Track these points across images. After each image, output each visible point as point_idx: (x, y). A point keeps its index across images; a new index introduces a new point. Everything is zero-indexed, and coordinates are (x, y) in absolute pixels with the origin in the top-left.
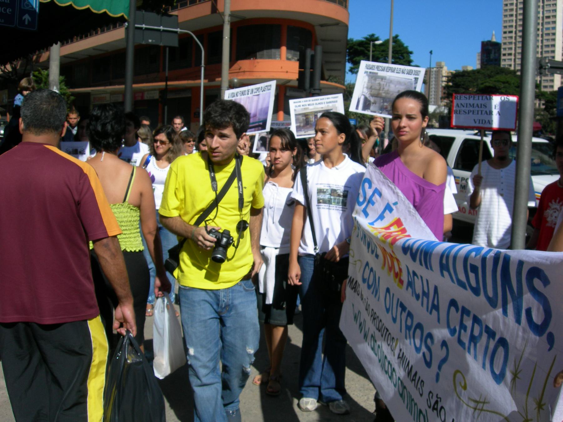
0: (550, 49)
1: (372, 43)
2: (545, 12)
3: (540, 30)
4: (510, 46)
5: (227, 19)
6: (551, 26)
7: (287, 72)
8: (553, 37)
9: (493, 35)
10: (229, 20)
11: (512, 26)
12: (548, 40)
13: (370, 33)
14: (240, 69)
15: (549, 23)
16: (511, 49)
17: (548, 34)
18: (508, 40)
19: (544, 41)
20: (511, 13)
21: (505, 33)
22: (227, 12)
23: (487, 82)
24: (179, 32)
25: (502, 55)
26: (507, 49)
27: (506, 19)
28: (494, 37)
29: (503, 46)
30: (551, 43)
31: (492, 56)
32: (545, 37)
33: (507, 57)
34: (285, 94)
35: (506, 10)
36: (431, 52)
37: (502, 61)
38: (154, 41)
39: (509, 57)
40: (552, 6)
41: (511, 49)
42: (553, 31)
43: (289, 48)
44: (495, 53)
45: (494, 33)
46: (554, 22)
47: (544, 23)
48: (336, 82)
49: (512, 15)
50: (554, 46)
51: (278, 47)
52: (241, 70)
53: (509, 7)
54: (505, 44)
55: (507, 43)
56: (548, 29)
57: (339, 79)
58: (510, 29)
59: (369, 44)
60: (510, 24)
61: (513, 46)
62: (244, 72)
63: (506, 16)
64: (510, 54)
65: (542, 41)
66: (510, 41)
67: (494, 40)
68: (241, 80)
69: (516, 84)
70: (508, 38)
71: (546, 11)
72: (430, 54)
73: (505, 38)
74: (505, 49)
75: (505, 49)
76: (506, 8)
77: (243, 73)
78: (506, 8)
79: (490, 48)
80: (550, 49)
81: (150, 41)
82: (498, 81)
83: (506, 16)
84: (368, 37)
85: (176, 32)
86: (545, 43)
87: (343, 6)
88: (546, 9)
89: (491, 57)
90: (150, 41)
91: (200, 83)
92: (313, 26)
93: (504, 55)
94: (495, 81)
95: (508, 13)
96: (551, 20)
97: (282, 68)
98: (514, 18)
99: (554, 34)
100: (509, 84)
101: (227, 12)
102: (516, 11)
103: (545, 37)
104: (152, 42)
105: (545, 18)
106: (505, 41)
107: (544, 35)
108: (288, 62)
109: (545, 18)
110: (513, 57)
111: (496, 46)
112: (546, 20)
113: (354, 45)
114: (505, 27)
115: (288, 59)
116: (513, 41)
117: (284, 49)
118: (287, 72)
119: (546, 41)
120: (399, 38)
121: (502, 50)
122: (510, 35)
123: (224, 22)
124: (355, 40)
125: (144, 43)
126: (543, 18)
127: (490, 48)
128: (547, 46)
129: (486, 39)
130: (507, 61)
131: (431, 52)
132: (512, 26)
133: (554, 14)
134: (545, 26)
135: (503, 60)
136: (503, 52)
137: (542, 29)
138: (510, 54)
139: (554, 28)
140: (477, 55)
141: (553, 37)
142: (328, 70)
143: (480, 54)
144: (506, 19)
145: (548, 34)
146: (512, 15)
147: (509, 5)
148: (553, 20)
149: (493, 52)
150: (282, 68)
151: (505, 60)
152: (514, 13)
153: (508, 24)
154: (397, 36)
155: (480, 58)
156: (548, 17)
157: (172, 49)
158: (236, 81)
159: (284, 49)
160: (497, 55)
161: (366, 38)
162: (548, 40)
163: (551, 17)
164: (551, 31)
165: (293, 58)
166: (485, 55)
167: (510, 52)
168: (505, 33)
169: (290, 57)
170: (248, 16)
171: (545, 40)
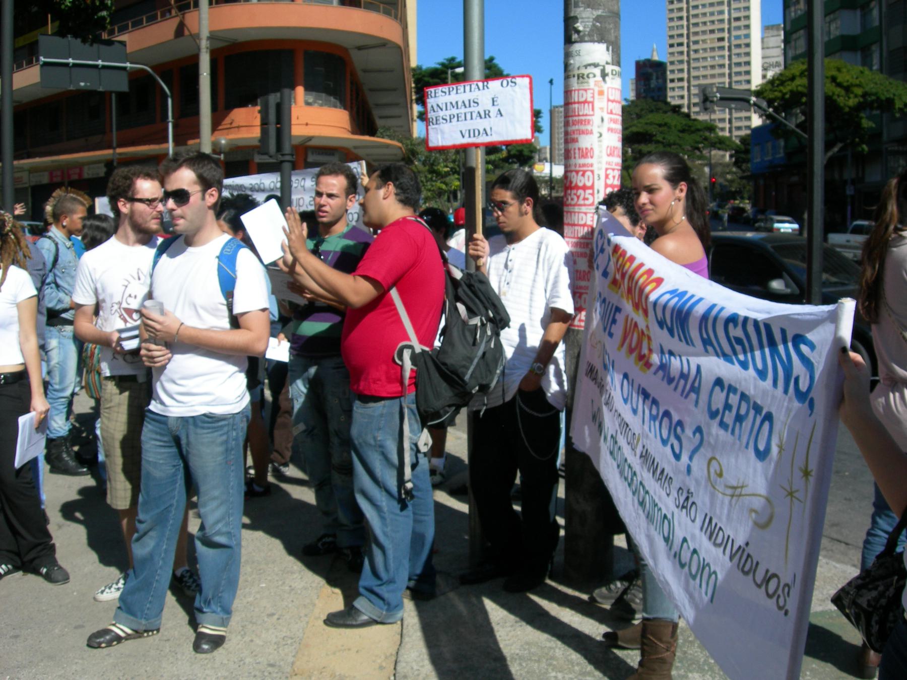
0: (743, 69)
1: (450, 71)
2: (732, 11)
3: (726, 40)
4: (680, 67)
5: (204, 44)
6: (742, 32)
7: (307, 124)
8: (747, 50)
9: (653, 51)
10: (208, 45)
11: (681, 35)
12: (738, 55)
13: (449, 56)
14: (231, 124)
15: (738, 28)
16: (681, 71)
17: (738, 46)
18: (677, 58)
19: (733, 57)
20: (680, 14)
21: (671, 46)
22: (205, 33)
23: (634, 125)
24: (128, 69)
25: (668, 81)
26: (676, 72)
27: (672, 24)
28: (655, 53)
29: (670, 67)
30: (743, 59)
31: (653, 83)
32: (735, 51)
33: (676, 84)
34: (305, 160)
35: (671, 11)
36: (551, 82)
37: (668, 90)
38: (88, 84)
39: (680, 84)
41: (681, 71)
42: (746, 41)
43: (309, 88)
44: (657, 78)
45: (655, 46)
46: (748, 27)
47: (732, 29)
48: (390, 137)
49: (681, 18)
50: (748, 63)
51: (293, 87)
52: (234, 125)
54: (672, 63)
57: (394, 132)
58: (680, 40)
59: (447, 73)
60: (680, 32)
61: (685, 66)
62: (238, 127)
63: (671, 19)
64: (681, 80)
65: (730, 57)
66: (680, 58)
67: (656, 58)
68: (231, 140)
69: (679, 127)
70: (676, 55)
71: (735, 9)
72: (549, 84)
73: (672, 54)
74: (672, 71)
75: (672, 71)
77: (236, 129)
79: (650, 70)
80: (743, 69)
81: (82, 84)
82: (651, 124)
83: (671, 19)
84: (445, 61)
85: (124, 69)
86: (735, 59)
87: (379, 11)
89: (652, 86)
90: (82, 84)
91: (168, 149)
92: (346, 50)
93: (672, 81)
94: (646, 124)
95: (675, 15)
96: (742, 23)
97: (298, 118)
98: (685, 23)
99: (748, 45)
100: (669, 127)
101: (205, 33)
102: (688, 11)
103: (735, 51)
104: (85, 85)
105: (732, 20)
106: (672, 59)
107: (733, 47)
108: (308, 109)
109: (732, 20)
110: (685, 84)
111: (659, 67)
112: (734, 24)
113: (424, 76)
114: (672, 37)
115: (308, 104)
116: (685, 58)
117: (300, 90)
118: (307, 124)
120: (495, 61)
121: (668, 73)
122: (680, 49)
123: (199, 49)
124: (424, 67)
125: (72, 88)
126: (729, 20)
127: (650, 70)
128: (738, 64)
129: (643, 57)
130: (677, 90)
131: (551, 82)
132: (681, 35)
133: (746, 14)
134: (734, 33)
135: (670, 88)
136: (670, 76)
137: (729, 39)
138: (681, 80)
139: (748, 36)
140: (630, 82)
141: (747, 50)
142: (381, 117)
143: (634, 81)
144: (672, 24)
145: (738, 46)
146: (681, 18)
148: (746, 23)
149: (654, 77)
150: (298, 118)
151: (673, 89)
152: (684, 14)
153: (675, 32)
154: (491, 59)
155: (634, 87)
156: (738, 19)
157: (120, 95)
158: (223, 142)
159: (300, 90)
160: (660, 81)
161: (443, 64)
162: (738, 55)
163: (743, 19)
164: (742, 41)
165: (315, 102)
166: (642, 83)
167: (680, 76)
168: (671, 46)
169: (311, 100)
170: (242, 38)
171: (735, 54)
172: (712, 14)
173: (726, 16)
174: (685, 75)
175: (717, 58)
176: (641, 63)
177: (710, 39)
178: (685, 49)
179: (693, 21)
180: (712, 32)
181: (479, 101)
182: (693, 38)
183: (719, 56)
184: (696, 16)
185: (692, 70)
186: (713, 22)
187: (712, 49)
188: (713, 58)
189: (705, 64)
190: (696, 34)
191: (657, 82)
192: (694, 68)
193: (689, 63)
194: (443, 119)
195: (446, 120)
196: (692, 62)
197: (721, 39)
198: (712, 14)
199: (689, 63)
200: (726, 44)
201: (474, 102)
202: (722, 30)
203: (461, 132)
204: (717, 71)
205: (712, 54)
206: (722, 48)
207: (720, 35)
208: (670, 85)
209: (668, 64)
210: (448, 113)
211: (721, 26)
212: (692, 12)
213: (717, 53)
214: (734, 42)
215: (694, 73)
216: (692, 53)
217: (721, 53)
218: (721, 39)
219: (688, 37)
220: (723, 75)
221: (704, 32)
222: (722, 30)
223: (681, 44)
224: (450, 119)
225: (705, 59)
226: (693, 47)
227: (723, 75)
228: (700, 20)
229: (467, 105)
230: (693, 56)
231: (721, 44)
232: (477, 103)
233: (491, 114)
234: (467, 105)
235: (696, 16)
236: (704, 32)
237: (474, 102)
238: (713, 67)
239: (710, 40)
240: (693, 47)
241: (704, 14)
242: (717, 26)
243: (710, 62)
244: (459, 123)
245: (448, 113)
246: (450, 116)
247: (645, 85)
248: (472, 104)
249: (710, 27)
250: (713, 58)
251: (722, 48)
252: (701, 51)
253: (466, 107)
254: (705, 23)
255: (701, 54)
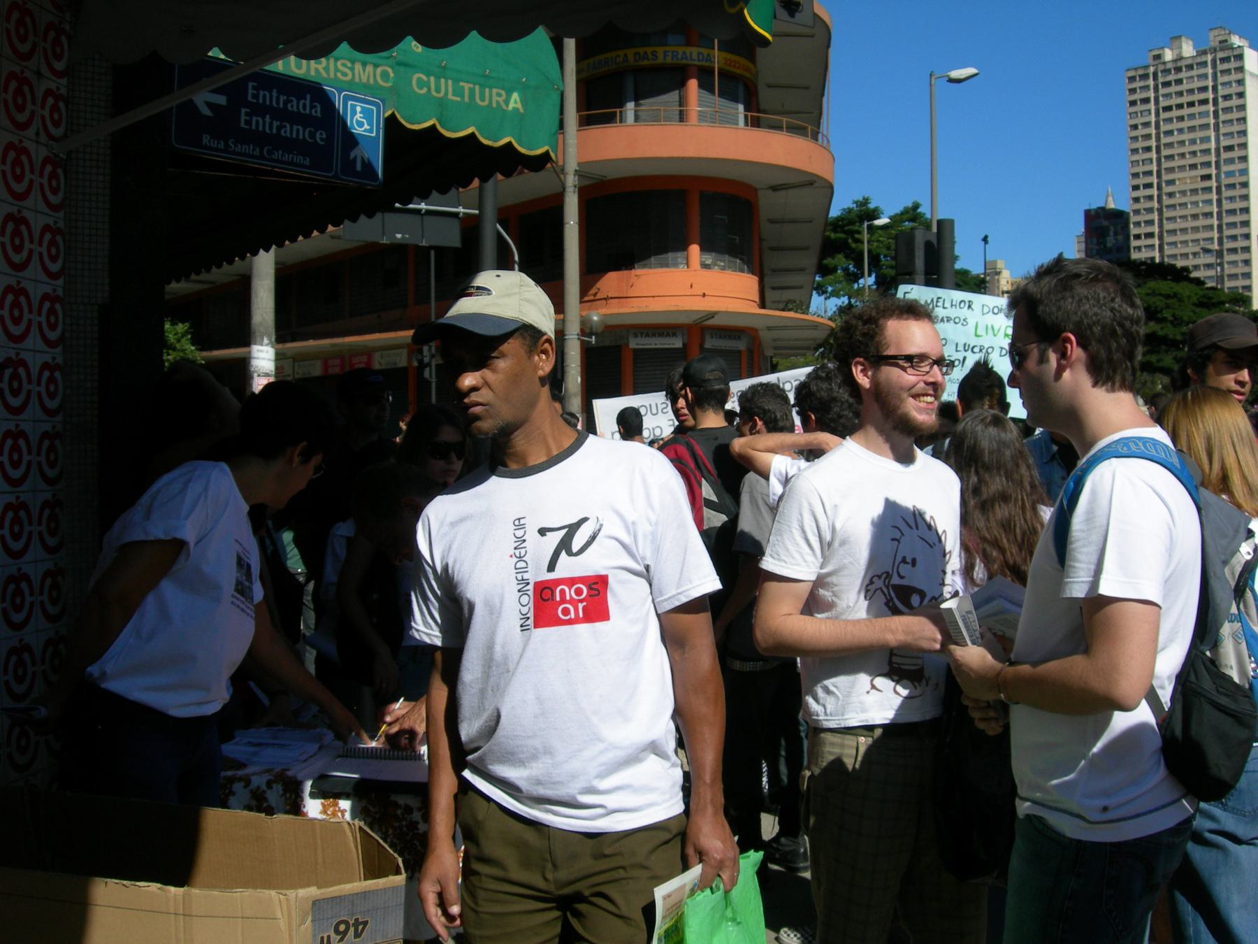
0: (1238, 218)
2: (1222, 138)
5: (571, 181)
8: (1243, 192)
11: (1150, 173)
12: (1231, 199)
15: (1230, 161)
16: (1150, 222)
17: (1232, 186)
18: (1143, 205)
19: (1224, 202)
20: (1146, 144)
21: (1136, 188)
22: (572, 165)
25: (1132, 238)
27: (1136, 157)
28: (1110, 199)
29: (1133, 219)
30: (1239, 205)
31: (1110, 242)
32: (1226, 193)
35: (1135, 139)
37: (1132, 250)
39: (1149, 242)
40: (1235, 123)
41: (1150, 222)
42: (1243, 179)
44: (1116, 234)
49: (1148, 149)
53: (1141, 131)
54: (1137, 212)
55: (1142, 211)
56: (1230, 174)
58: (1147, 180)
60: (1147, 168)
61: (1156, 217)
63: (1135, 151)
64: (1150, 235)
65: (1219, 202)
66: (1148, 205)
69: (1195, 299)
73: (1136, 200)
74: (1138, 224)
75: (1138, 224)
76: (1134, 133)
78: (1134, 133)
79: (1105, 223)
80: (1238, 218)
83: (1135, 151)
86: (1227, 205)
88: (1223, 130)
89: (1109, 245)
92: (754, 190)
93: (1138, 237)
95: (1140, 144)
96: (1236, 154)
98: (1154, 155)
100: (1180, 300)
101: (572, 165)
102: (1158, 139)
103: (1226, 193)
105: (1222, 150)
106: (1137, 206)
109: (1222, 150)
110: (1156, 242)
111: (1119, 217)
112: (1224, 156)
114: (1135, 175)
119: (1229, 202)
122: (1148, 192)
126: (1218, 150)
127: (1105, 223)
128: (1232, 212)
129: (1095, 205)
130: (1143, 250)
132: (1150, 173)
133: (1241, 141)
134: (1224, 168)
135: (1135, 248)
136: (1134, 231)
137: (1218, 175)
138: (1150, 235)
141: (1243, 192)
143: (1083, 239)
144: (1136, 157)
145: (1232, 186)
146: (1148, 149)
147: (1140, 127)
148: (1241, 153)
149: (1112, 233)
151: (1139, 248)
152: (1153, 143)
153: (1140, 169)
155: (1083, 246)
156: (1229, 148)
160: (1120, 238)
162: (1231, 199)
164: (1238, 179)
166: (1095, 241)
167: (1149, 230)
168: (1136, 188)
172: (1193, 142)
173: (1213, 145)
174: (1156, 229)
175: (1201, 205)
176: (1093, 213)
177: (1191, 178)
178: (1155, 192)
179: (1165, 152)
180: (1193, 167)
182: (1165, 177)
183: (1203, 202)
184: (1170, 145)
185: (1165, 222)
186: (1194, 153)
187: (1194, 191)
188: (1195, 203)
189: (1183, 212)
190: (1171, 170)
191: (1116, 239)
192: (1168, 219)
193: (1160, 211)
196: (1165, 210)
197: (1207, 177)
198: (1193, 142)
199: (1160, 211)
200: (1214, 184)
202: (1208, 164)
204: (1201, 222)
205: (1194, 198)
206: (1209, 189)
207: (1205, 172)
208: (1134, 243)
209: (1132, 214)
211: (1205, 159)
212: (1164, 140)
213: (1201, 197)
214: (1225, 181)
215: (1168, 226)
216: (1164, 197)
217: (1206, 197)
218: (1207, 177)
219: (1159, 176)
220: (1211, 227)
221: (1182, 168)
222: (1208, 164)
223: (1149, 186)
225: (1184, 205)
226: (1166, 189)
227: (1211, 227)
228: (1177, 150)
230: (1166, 201)
231: (1206, 184)
235: (1170, 145)
236: (1182, 168)
238: (1195, 217)
239: (1187, 180)
240: (1166, 189)
241: (1182, 143)
242: (1199, 159)
243: (1190, 210)
247: (1098, 244)
249: (1190, 160)
250: (1195, 203)
251: (1209, 189)
252: (1178, 195)
254: (1182, 155)
255: (1178, 199)
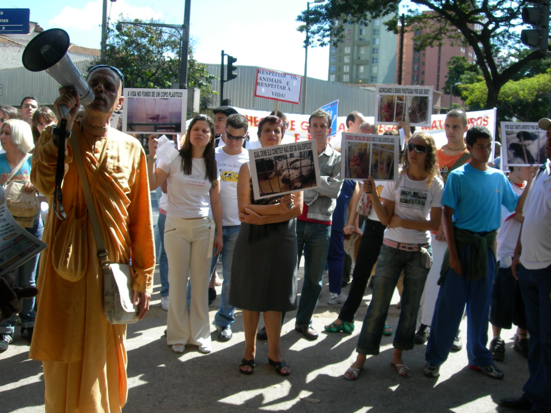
181: (282, 82)
194: (265, 85)
195: (267, 85)
201: (280, 81)
203: (273, 92)
210: (268, 83)
224: (269, 86)
229: (277, 82)
232: (281, 82)
233: (286, 88)
234: (277, 82)
237: (280, 81)
244: (272, 88)
245: (268, 83)
246: (269, 84)
248: (279, 82)
253: (276, 82)
